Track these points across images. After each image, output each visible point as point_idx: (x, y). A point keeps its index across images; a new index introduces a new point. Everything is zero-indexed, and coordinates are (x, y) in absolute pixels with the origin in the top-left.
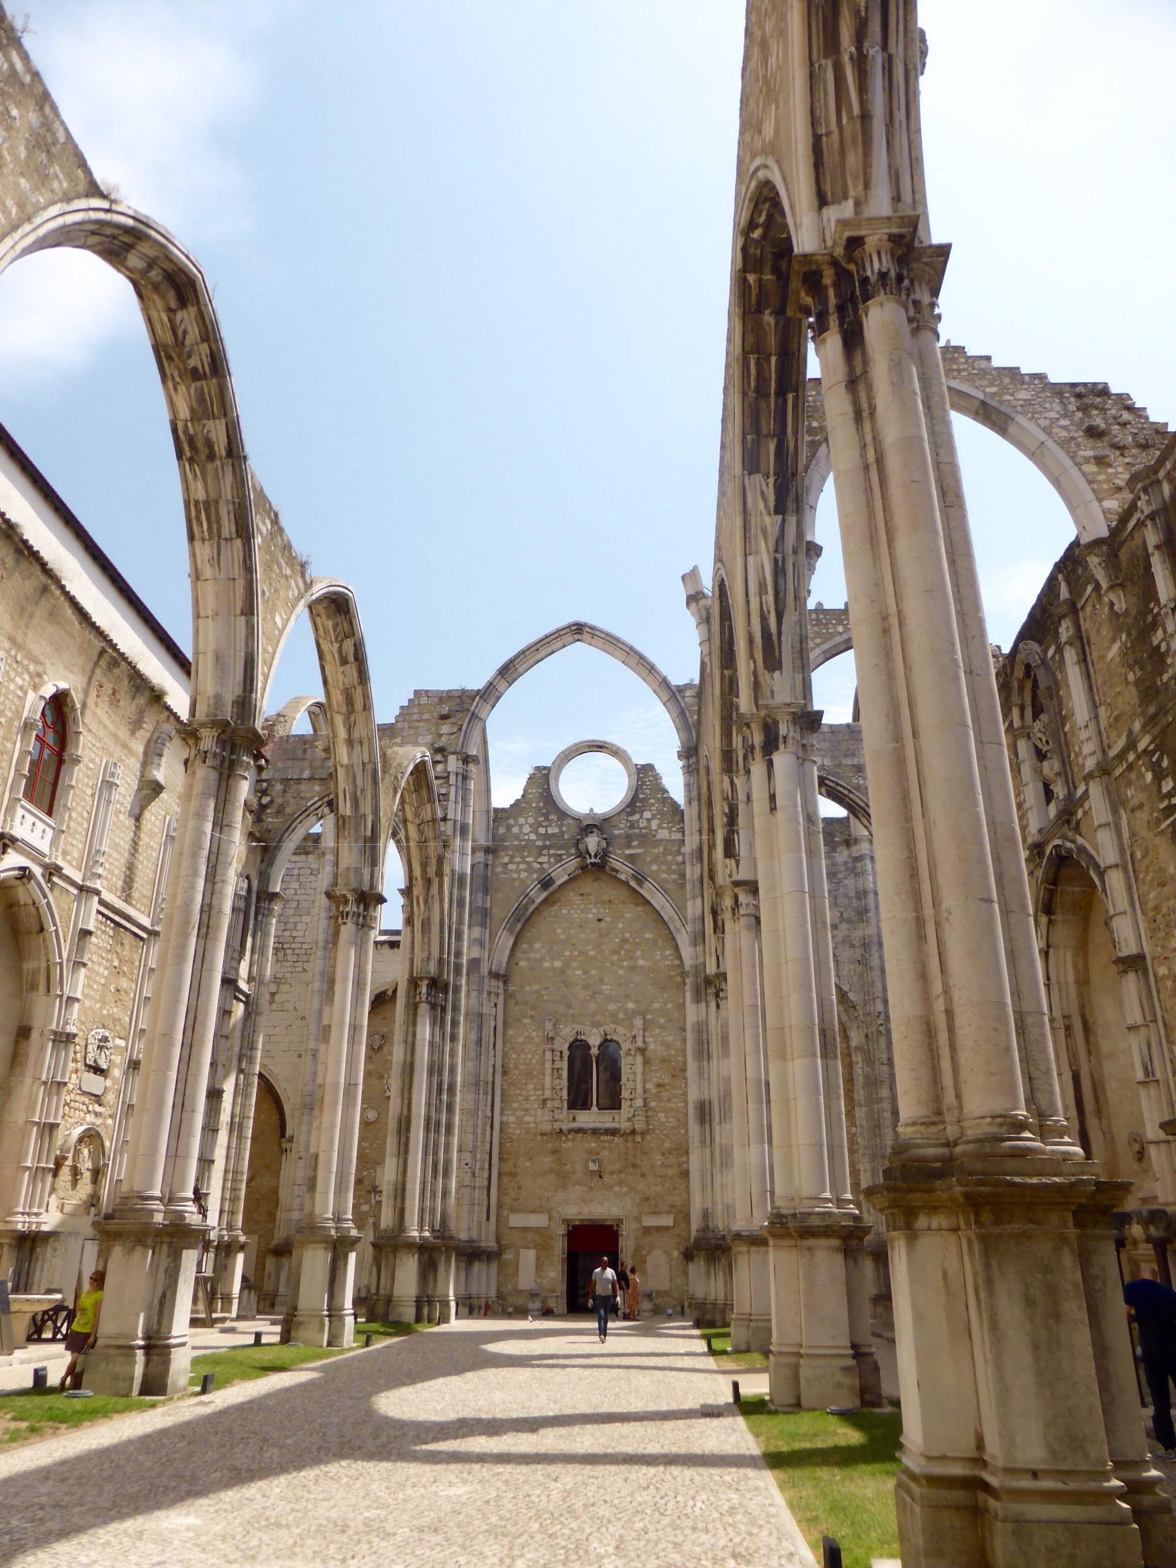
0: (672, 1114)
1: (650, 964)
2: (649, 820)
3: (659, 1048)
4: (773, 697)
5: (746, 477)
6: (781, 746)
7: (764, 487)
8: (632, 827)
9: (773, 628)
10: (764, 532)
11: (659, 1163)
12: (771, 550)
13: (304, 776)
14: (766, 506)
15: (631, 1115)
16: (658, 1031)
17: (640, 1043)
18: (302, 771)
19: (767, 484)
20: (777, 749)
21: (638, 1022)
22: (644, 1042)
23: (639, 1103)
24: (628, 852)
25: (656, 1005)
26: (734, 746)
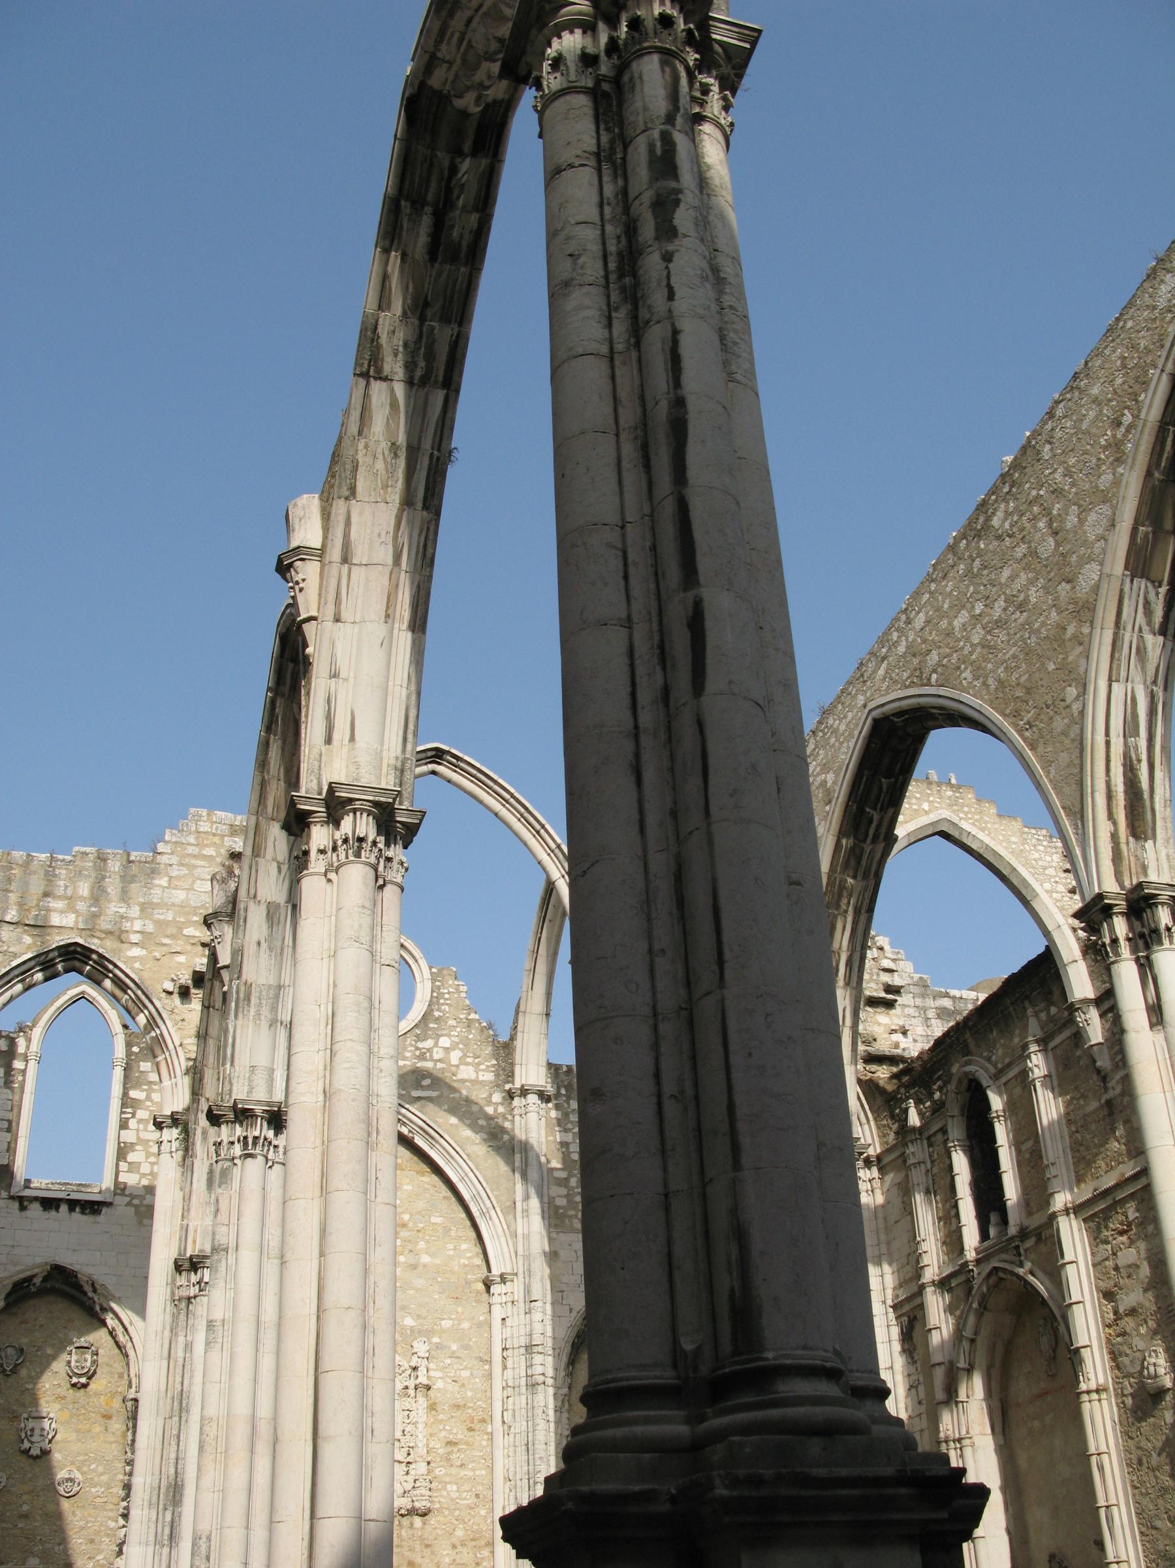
0: (467, 1487)
1: (437, 1261)
2: (446, 1049)
3: (450, 1387)
4: (1146, 875)
5: (1128, 580)
6: (1166, 942)
7: (1152, 596)
8: (422, 1057)
9: (1145, 785)
10: (1141, 652)
11: (447, 1560)
12: (1149, 680)
13: (8, 919)
14: (1149, 623)
15: (408, 1486)
16: (448, 1361)
17: (422, 1379)
18: (5, 910)
19: (1157, 594)
20: (1160, 943)
21: (421, 1348)
22: (429, 1378)
23: (421, 1468)
24: (415, 1094)
25: (447, 1324)
26: (836, 946)
